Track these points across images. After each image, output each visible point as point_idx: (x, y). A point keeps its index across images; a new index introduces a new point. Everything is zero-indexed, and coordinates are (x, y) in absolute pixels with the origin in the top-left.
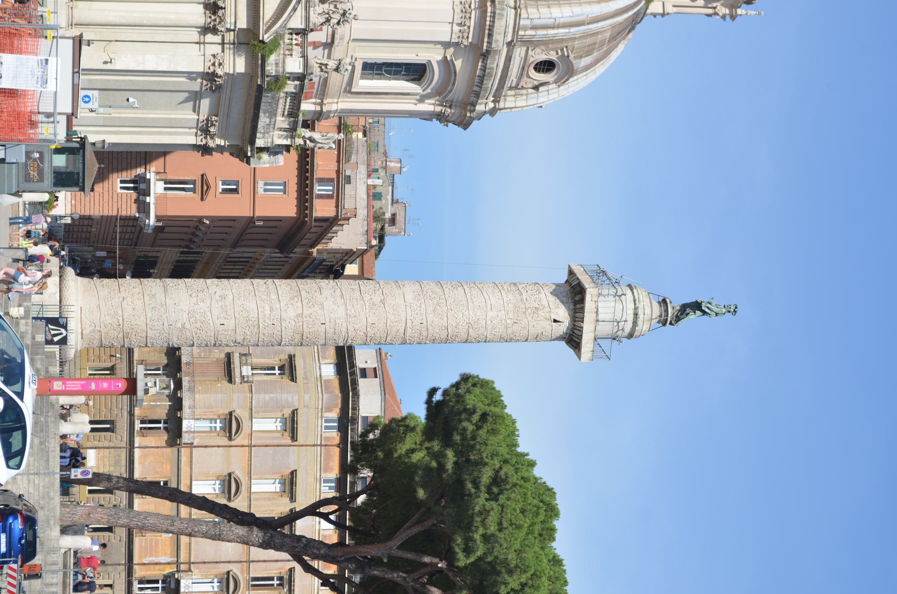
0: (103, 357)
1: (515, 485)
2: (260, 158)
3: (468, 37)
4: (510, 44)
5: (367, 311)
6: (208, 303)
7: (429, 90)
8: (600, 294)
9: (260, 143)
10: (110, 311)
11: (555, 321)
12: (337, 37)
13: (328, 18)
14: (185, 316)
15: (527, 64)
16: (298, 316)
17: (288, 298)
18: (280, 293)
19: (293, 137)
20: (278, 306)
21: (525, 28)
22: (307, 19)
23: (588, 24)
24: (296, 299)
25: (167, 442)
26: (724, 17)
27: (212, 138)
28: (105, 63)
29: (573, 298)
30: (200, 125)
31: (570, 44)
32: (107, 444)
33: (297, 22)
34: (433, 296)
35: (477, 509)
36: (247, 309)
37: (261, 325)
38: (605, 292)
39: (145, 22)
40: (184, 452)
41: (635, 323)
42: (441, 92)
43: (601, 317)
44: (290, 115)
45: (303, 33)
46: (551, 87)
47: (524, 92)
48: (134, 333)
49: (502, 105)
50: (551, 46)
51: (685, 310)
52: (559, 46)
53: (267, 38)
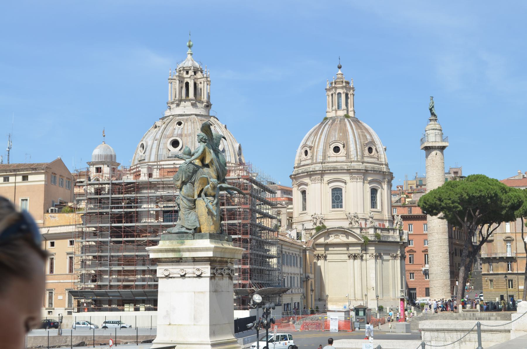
0: (487, 284)
1: (440, 195)
2: (404, 239)
4: (363, 163)
7: (380, 187)
8: (428, 141)
9: (399, 240)
11: (436, 154)
12: (363, 218)
14: (439, 268)
16: (437, 234)
19: (396, 229)
21: (358, 158)
22: (357, 228)
23: (355, 138)
25: (515, 262)
26: (354, 91)
27: (398, 255)
28: (373, 290)
29: (429, 149)
30: (393, 259)
31: (362, 143)
32: (517, 282)
33: (358, 231)
35: (445, 206)
38: (427, 139)
39: (360, 277)
40: (518, 256)
41: (436, 129)
42: (380, 183)
43: (434, 140)
44: (389, 231)
45: (361, 229)
46: (377, 147)
47: (379, 156)
49: (384, 163)
50: (363, 149)
51: (433, 114)
52: (363, 147)
53: (363, 240)
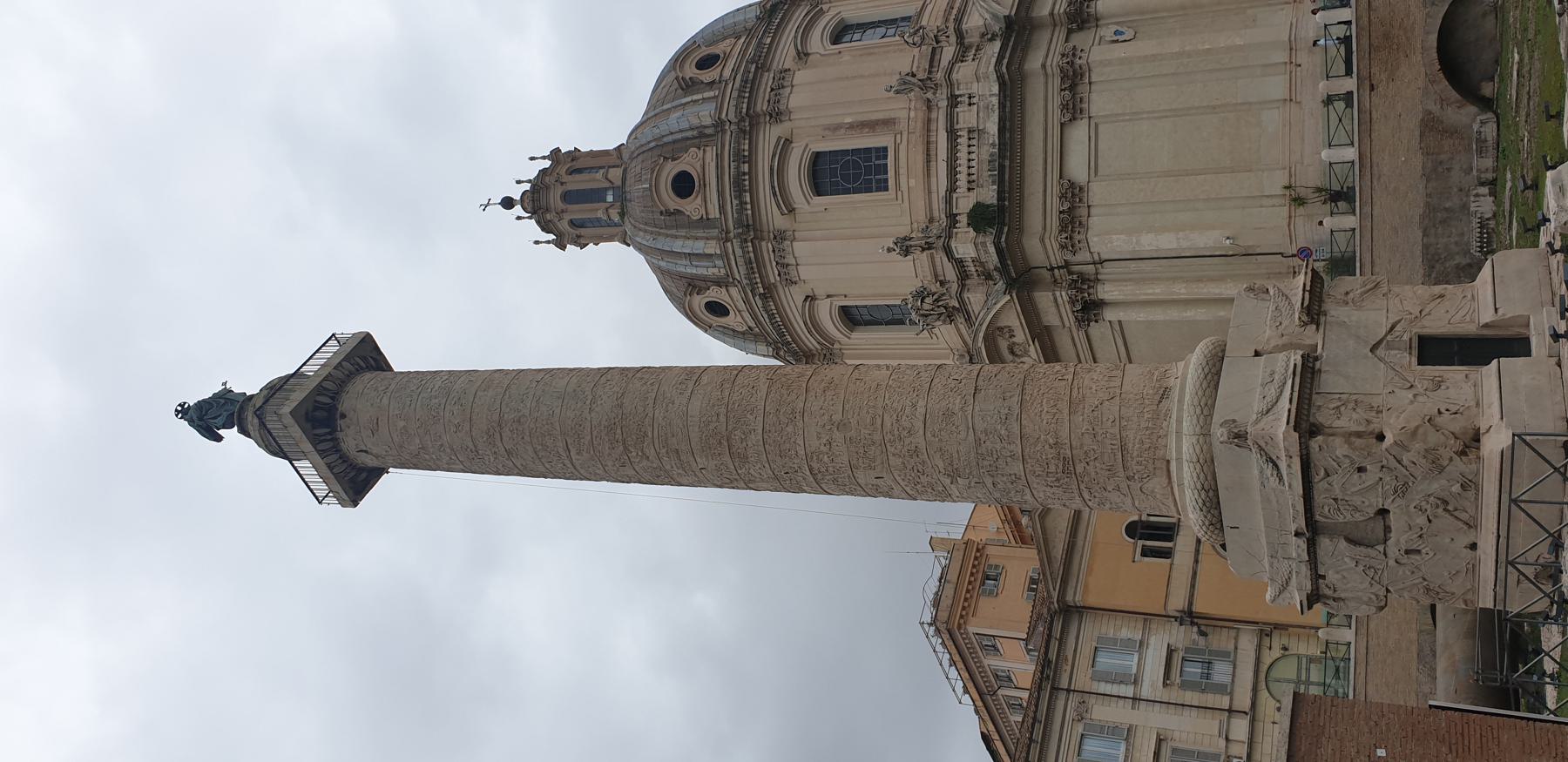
15: (702, 191)
48: (1052, 468)
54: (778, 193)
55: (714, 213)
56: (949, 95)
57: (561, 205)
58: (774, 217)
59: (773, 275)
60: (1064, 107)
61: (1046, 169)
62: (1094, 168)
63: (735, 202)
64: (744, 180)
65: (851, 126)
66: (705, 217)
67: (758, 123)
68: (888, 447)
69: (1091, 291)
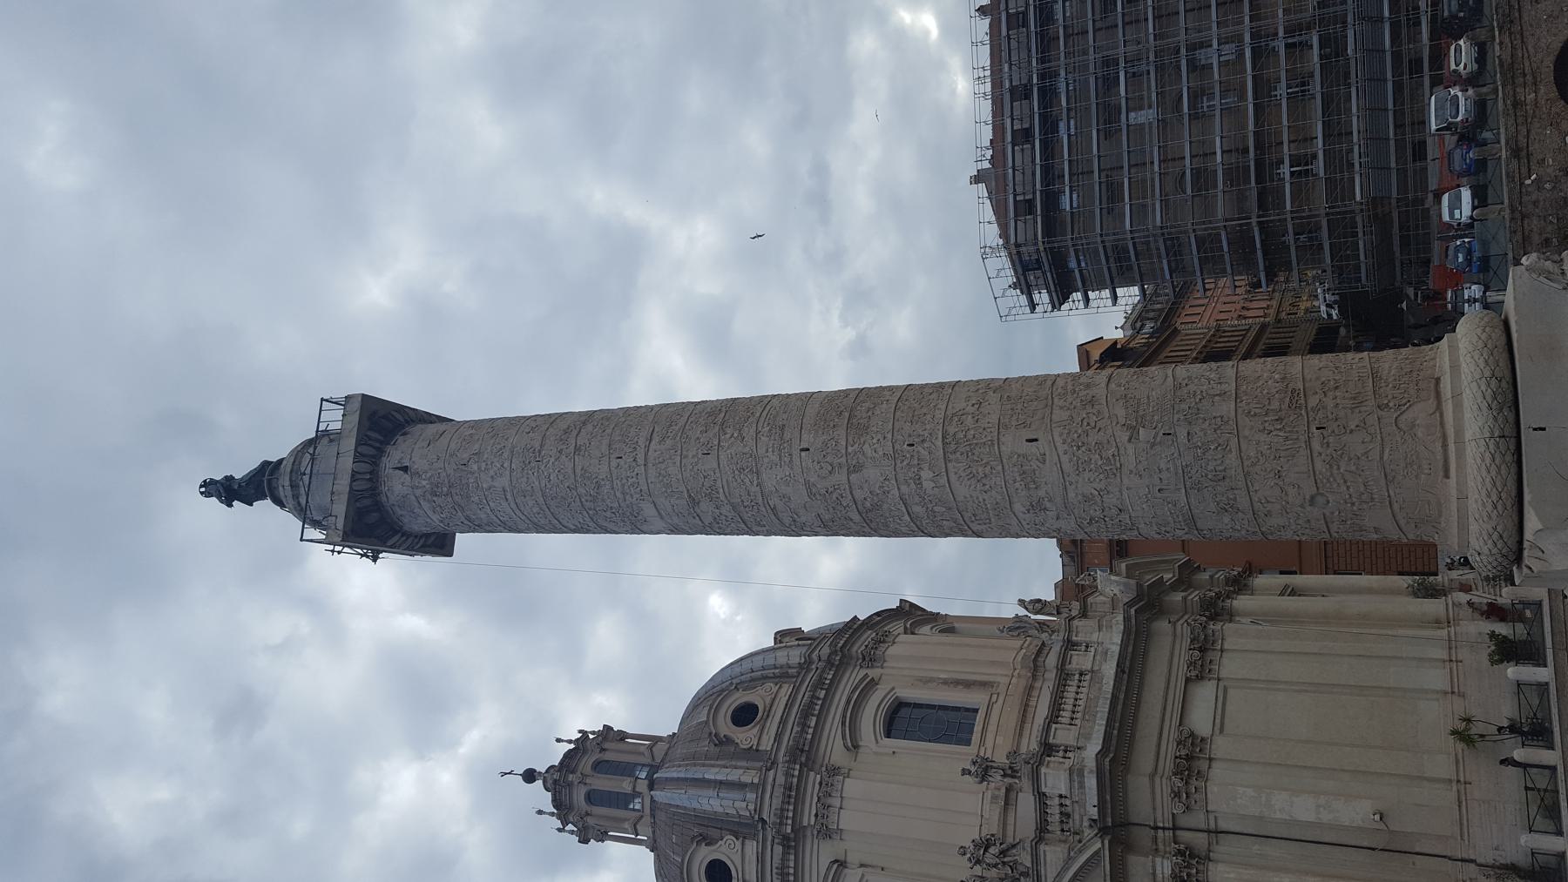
3: (821, 784)
5: (719, 484)
6: (1071, 495)
10: (1353, 468)
11: (405, 469)
13: (1004, 857)
16: (857, 468)
17: (885, 506)
18: (907, 517)
20: (904, 488)
24: (868, 504)
34: (608, 514)
36: (973, 481)
37: (939, 443)
48: (1275, 405)
54: (847, 724)
55: (767, 744)
56: (1043, 741)
57: (588, 770)
58: (833, 748)
59: (808, 818)
60: (1191, 664)
61: (1164, 715)
62: (1220, 726)
63: (796, 729)
64: (816, 704)
65: (945, 682)
66: (754, 747)
67: (848, 664)
68: (1056, 400)
69: (1201, 867)
